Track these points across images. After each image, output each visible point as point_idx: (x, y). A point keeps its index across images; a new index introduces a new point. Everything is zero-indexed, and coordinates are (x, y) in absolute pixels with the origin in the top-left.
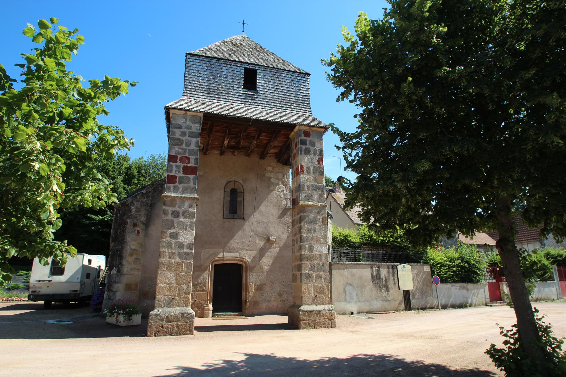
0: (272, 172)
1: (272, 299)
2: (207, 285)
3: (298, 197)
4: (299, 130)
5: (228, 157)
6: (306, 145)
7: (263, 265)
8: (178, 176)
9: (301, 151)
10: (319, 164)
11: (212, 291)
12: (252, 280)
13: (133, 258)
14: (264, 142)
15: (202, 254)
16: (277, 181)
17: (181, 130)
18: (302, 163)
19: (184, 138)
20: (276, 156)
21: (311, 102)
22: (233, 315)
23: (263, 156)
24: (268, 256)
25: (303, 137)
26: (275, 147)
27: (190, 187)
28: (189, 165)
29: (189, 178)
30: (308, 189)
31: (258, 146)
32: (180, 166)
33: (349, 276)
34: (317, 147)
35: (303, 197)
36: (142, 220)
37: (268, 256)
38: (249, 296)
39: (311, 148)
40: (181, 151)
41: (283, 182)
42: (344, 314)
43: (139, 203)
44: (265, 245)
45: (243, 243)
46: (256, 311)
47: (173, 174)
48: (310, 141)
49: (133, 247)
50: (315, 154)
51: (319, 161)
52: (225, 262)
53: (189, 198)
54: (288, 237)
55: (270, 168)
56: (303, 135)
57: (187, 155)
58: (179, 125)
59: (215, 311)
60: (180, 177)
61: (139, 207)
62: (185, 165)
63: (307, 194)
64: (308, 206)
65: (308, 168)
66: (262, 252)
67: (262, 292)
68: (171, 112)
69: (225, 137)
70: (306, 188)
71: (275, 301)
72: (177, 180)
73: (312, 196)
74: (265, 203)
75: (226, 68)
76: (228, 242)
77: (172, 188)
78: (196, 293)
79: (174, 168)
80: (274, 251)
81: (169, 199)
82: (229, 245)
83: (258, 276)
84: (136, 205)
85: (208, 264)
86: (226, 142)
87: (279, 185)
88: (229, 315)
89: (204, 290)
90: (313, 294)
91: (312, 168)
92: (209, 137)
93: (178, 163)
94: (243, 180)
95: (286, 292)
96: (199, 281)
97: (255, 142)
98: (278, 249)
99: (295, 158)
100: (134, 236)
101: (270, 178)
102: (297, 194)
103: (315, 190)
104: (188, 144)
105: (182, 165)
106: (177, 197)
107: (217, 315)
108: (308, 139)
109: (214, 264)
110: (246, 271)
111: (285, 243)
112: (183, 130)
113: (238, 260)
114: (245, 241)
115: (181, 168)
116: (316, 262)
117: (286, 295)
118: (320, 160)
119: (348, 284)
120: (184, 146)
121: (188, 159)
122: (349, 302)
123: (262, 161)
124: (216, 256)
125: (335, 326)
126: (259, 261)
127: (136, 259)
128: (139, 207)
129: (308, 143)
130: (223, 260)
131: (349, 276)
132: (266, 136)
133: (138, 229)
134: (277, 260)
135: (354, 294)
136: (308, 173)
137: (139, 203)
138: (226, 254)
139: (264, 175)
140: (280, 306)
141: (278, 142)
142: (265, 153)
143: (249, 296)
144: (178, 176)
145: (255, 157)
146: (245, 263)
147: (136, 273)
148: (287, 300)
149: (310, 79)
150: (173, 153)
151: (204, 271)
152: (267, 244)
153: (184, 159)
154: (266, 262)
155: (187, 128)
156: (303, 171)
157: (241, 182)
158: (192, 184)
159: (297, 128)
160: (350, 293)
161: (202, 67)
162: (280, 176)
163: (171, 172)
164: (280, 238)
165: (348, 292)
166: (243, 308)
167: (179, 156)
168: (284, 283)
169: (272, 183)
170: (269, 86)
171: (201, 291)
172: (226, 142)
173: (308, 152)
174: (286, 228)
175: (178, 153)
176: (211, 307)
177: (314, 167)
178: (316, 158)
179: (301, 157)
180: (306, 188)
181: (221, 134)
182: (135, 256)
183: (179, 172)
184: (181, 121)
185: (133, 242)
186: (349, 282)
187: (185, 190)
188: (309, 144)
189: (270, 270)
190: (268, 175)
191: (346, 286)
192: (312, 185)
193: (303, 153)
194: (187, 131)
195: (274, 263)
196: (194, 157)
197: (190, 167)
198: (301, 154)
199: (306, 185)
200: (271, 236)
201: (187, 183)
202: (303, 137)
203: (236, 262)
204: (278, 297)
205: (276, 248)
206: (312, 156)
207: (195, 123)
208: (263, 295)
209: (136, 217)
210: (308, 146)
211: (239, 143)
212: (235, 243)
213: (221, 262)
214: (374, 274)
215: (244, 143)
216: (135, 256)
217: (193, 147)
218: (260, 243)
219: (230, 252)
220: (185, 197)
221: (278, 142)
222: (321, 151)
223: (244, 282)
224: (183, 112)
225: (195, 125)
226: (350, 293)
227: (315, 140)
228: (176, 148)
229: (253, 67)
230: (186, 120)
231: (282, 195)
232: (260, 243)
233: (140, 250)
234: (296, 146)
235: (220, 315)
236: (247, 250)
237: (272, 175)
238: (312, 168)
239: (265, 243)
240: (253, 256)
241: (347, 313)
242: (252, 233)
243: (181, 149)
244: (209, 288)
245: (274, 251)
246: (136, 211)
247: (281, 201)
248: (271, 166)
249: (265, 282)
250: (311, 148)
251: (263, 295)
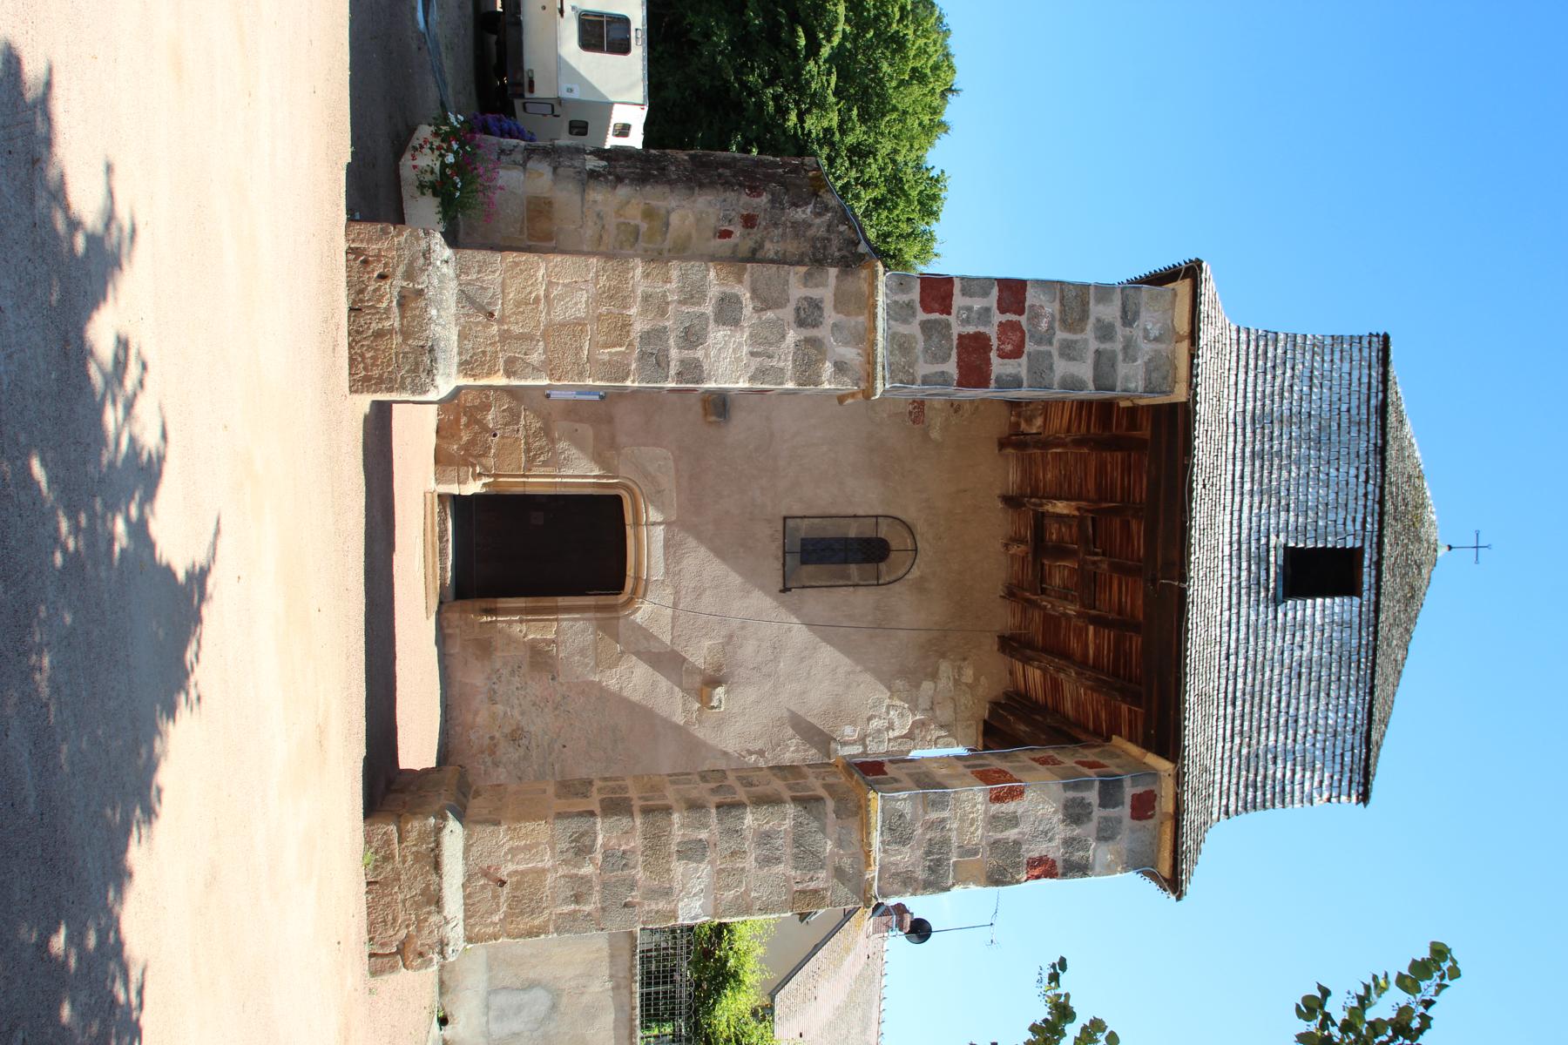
0: (957, 682)
1: (500, 708)
2: (548, 470)
3: (894, 784)
4: (1154, 774)
5: (996, 524)
6: (1103, 805)
7: (622, 668)
8: (952, 319)
9: (1076, 786)
10: (1032, 864)
11: (530, 490)
12: (567, 629)
13: (638, 221)
14: (1074, 644)
15: (658, 451)
16: (924, 702)
17: (1118, 324)
18: (1029, 795)
19: (1089, 333)
20: (1017, 693)
21: (1261, 813)
22: (443, 569)
23: (1011, 645)
24: (654, 684)
25: (1129, 791)
26: (1056, 686)
27: (911, 365)
28: (993, 355)
29: (945, 359)
30: (931, 826)
31: (1052, 623)
32: (987, 323)
33: (585, 999)
34: (1101, 853)
35: (899, 805)
36: (768, 245)
37: (654, 684)
38: (510, 623)
39: (1091, 827)
40: (1044, 325)
41: (921, 724)
42: (443, 987)
43: (822, 232)
44: (694, 670)
45: (699, 592)
46: (455, 649)
47: (958, 300)
48: (1119, 821)
49: (675, 219)
50: (1068, 842)
51: (1041, 861)
52: (630, 531)
53: (871, 361)
54: (725, 754)
55: (968, 675)
56: (1140, 790)
57: (1029, 346)
58: (1136, 315)
59: (461, 506)
60: (948, 326)
61: (811, 232)
62: (994, 342)
63: (912, 823)
64: (865, 827)
65: (1013, 820)
66: (668, 662)
67: (525, 668)
68: (1183, 287)
69: (1079, 498)
70: (934, 816)
71: (494, 716)
72: (935, 316)
73: (903, 841)
74: (845, 663)
75: (1352, 481)
76: (700, 537)
77: (905, 298)
78: (521, 434)
79: (977, 304)
80: (672, 704)
81: (865, 287)
82: (692, 542)
83: (582, 652)
84: (818, 221)
85: (622, 471)
86: (1061, 507)
87: (913, 710)
88: (442, 552)
89: (531, 461)
90: (511, 867)
91: (1012, 834)
92: (1079, 443)
93: (998, 318)
94: (922, 578)
95: (525, 758)
96: (562, 445)
97: (1072, 610)
98: (679, 719)
99: (1043, 762)
100: (712, 221)
101: (934, 676)
102: (907, 782)
103: (929, 853)
104: (1068, 351)
105: (992, 332)
106: (875, 316)
107: (443, 511)
108: (1125, 810)
109: (623, 493)
110: (598, 608)
111: (704, 744)
112: (1120, 332)
113: (637, 578)
114: (707, 598)
115: (981, 329)
116: (640, 874)
117: (515, 756)
118: (1045, 868)
119: (556, 995)
120: (1060, 335)
121: (1017, 353)
122: (488, 1007)
123: (991, 644)
124: (649, 500)
125: (375, 973)
126: (638, 654)
127: (636, 232)
128: (811, 232)
129: (1111, 812)
130: (637, 523)
131: (585, 999)
132: (1098, 648)
133: (738, 230)
134: (642, 715)
135: (516, 1026)
136: (994, 821)
137: (822, 232)
138: (659, 532)
139: (943, 655)
140: (473, 737)
141: (1075, 692)
142: (1028, 652)
143: (510, 623)
144: (952, 319)
145: (1005, 618)
146: (630, 601)
147: (589, 232)
148: (496, 764)
149: (1348, 805)
150: (1032, 297)
151: (598, 458)
152: (698, 679)
153: (1015, 337)
154: (633, 679)
155: (1128, 345)
156: (998, 798)
157: (915, 573)
158: (923, 369)
159: (1164, 766)
160: (519, 1009)
161: (1344, 392)
162: (945, 714)
163: (964, 293)
164: (720, 724)
165: (526, 997)
166: (468, 604)
167: (1023, 319)
168: (557, 746)
169: (918, 686)
170: (1307, 646)
171: (528, 450)
172: (1061, 507)
173: (1075, 813)
174: (758, 745)
175: (1036, 316)
176: (473, 488)
177: (1017, 843)
178: (1053, 850)
179: (1055, 786)
180: (934, 816)
181: (1091, 485)
182: (644, 227)
183: (967, 321)
184: (1150, 320)
185: (691, 218)
186: (565, 1000)
187: (900, 344)
188: (1106, 819)
189: (604, 695)
190: (945, 667)
191: (546, 988)
192: (945, 842)
193: (1071, 794)
194: (1117, 346)
195: (632, 707)
196: (1024, 373)
197: (988, 362)
198: (1066, 787)
199: (946, 814)
200: (727, 692)
201: (926, 350)
202: (1129, 791)
203: (630, 572)
204: (507, 730)
205: (686, 711)
206: (1062, 831)
207: (1148, 372)
208: (513, 673)
209: (776, 225)
210: (1098, 813)
211: (1061, 551)
212: (699, 561)
213: (629, 518)
215: (1060, 572)
216: (644, 227)
217: (1061, 367)
218: (700, 654)
219: (666, 546)
220: (874, 344)
221: (1075, 692)
222: (1079, 869)
223: (562, 601)
224: (1183, 327)
225: (1141, 373)
226: (519, 1009)
227: (1124, 841)
228: (1051, 308)
229: (1367, 579)
230: (1156, 339)
231: (875, 724)
232: (700, 654)
233: (668, 244)
234: (1091, 765)
235: (443, 522)
236: (675, 606)
237: (945, 683)
238: (1012, 834)
239: (701, 672)
240: (654, 630)
241: (447, 999)
242: (736, 623)
243: (1051, 327)
244: (540, 481)
245: (672, 704)
246: (795, 225)
247: (853, 723)
248: (977, 679)
249: (561, 679)
250: (1091, 827)
251: (513, 673)
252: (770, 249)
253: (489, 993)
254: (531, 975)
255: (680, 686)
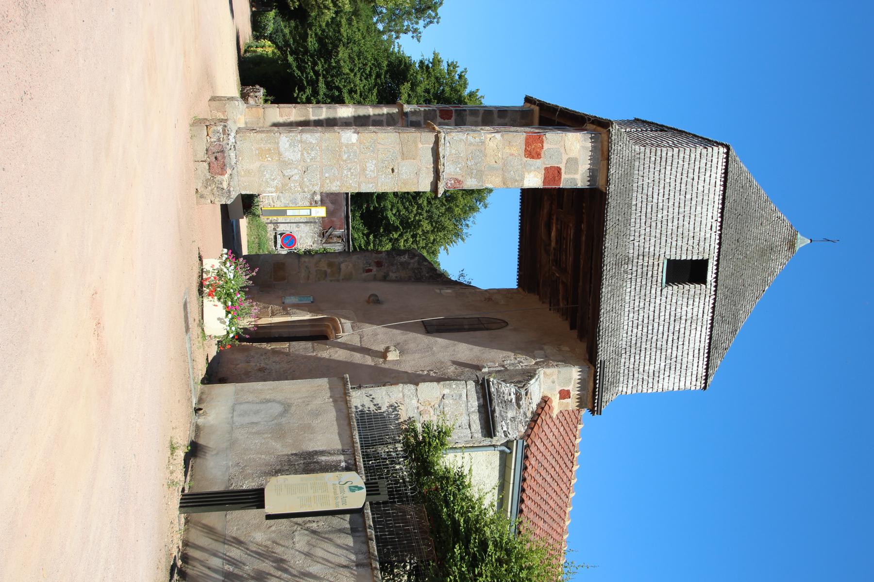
13: (326, 268)
36: (391, 274)
43: (416, 265)
44: (377, 351)
49: (343, 266)
84: (412, 261)
127: (325, 272)
133: (375, 269)
137: (416, 265)
154: (340, 355)
165: (263, 406)
182: (329, 271)
185: (351, 265)
186: (293, 409)
191: (279, 402)
209: (392, 265)
214: (323, 458)
216: (329, 271)
233: (341, 278)
246: (402, 264)
247: (494, 362)
252: (393, 275)
253: (235, 404)
254: (268, 397)
255: (369, 355)
